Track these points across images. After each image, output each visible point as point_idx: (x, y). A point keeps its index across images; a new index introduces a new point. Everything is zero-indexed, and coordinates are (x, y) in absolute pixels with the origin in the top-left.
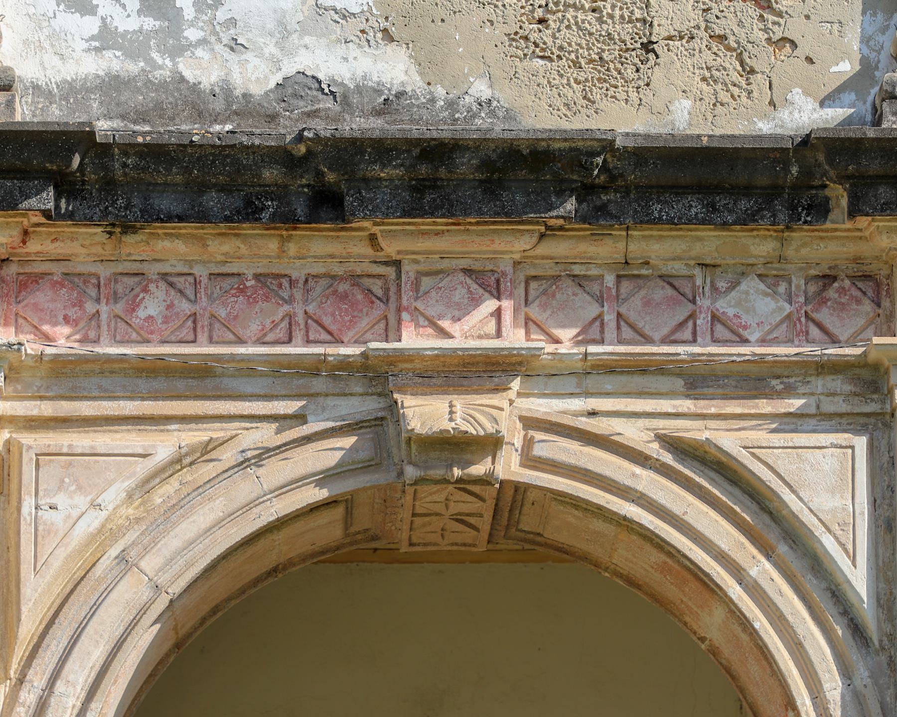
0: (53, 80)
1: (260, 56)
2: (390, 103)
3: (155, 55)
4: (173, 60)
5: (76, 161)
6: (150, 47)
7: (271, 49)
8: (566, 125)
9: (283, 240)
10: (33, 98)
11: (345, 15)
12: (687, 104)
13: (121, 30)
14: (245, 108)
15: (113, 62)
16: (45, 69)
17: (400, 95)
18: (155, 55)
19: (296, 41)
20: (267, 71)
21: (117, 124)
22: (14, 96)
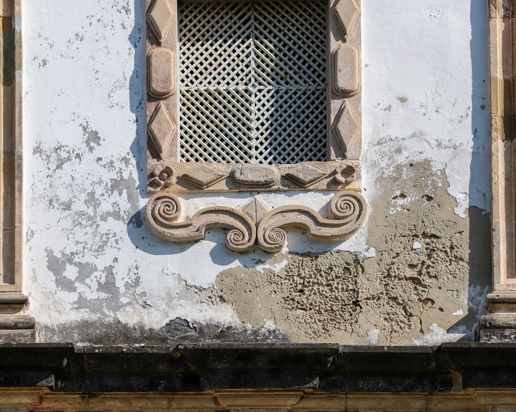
1: (158, 310)
2: (225, 332)
3: (106, 311)
4: (114, 313)
5: (65, 362)
6: (103, 307)
7: (164, 306)
8: (313, 342)
9: (170, 400)
11: (201, 289)
12: (377, 331)
13: (88, 299)
14: (151, 335)
15: (84, 315)
17: (229, 328)
18: (106, 311)
19: (176, 303)
20: (162, 317)
21: (87, 344)
22: (35, 331)
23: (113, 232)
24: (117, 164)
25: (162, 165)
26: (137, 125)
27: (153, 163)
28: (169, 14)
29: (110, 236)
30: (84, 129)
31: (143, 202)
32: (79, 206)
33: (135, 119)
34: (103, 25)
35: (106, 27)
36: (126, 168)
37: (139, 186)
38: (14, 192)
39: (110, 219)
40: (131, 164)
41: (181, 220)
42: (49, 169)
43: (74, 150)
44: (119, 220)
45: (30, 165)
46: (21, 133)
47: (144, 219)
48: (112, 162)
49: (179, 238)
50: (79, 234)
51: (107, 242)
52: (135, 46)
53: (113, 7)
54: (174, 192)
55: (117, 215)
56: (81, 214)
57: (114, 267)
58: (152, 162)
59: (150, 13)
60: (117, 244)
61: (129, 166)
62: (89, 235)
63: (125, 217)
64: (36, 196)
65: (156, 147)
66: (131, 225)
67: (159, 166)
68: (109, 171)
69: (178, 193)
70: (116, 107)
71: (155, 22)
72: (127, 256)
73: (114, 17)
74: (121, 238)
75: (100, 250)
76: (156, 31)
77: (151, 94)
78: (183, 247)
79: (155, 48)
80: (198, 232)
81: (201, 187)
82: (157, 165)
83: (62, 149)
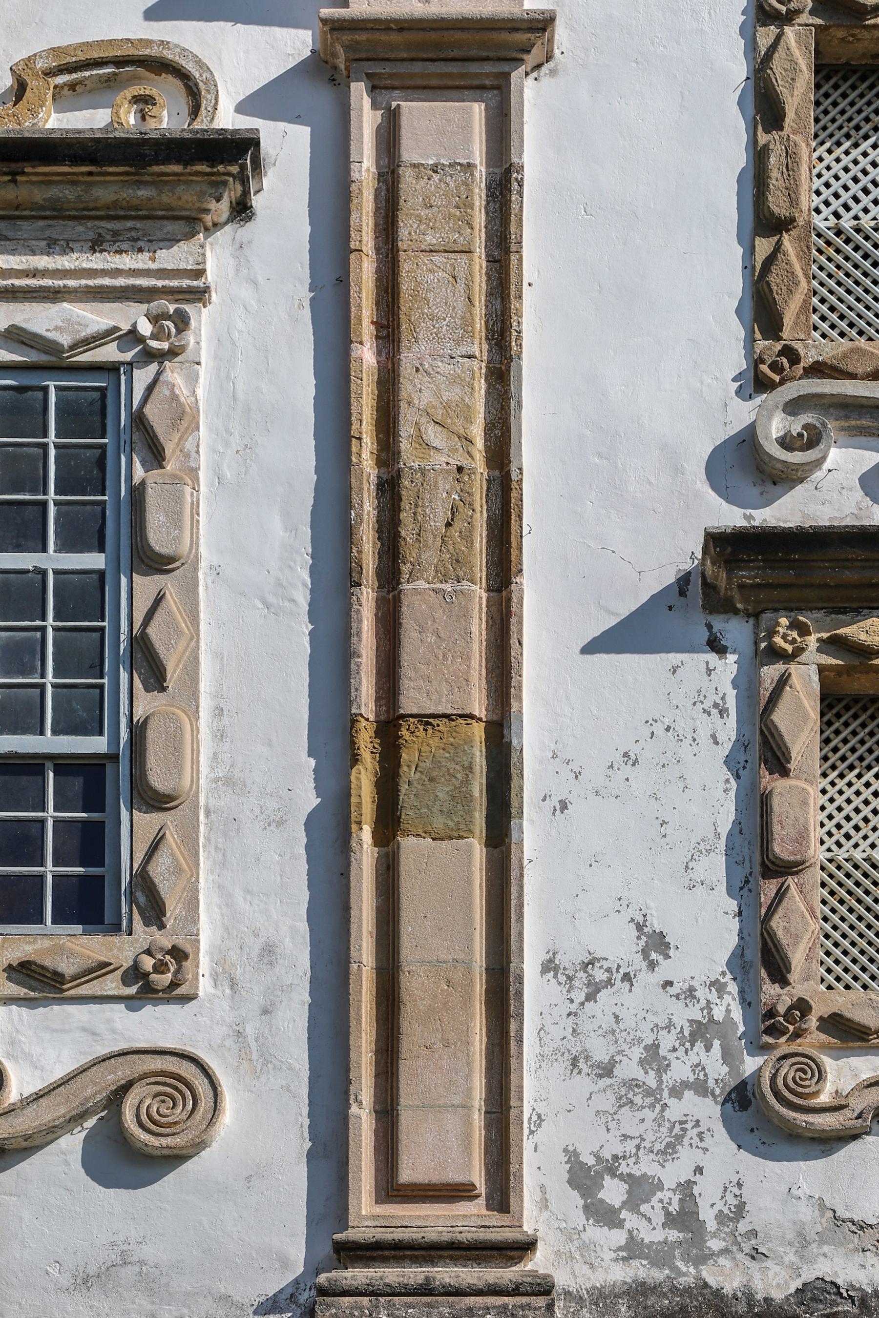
0: (583, 1287)
1: (781, 1263)
3: (680, 1264)
4: (696, 1268)
6: (674, 1257)
7: (791, 1257)
10: (565, 1303)
13: (646, 1241)
15: (640, 1270)
16: (575, 1277)
18: (680, 1264)
19: (815, 1250)
20: (787, 1277)
23: (694, 1119)
24: (702, 993)
25: (791, 996)
26: (741, 922)
27: (772, 991)
28: (806, 718)
29: (688, 1126)
30: (640, 928)
31: (751, 1064)
32: (629, 1069)
33: (737, 909)
34: (677, 738)
35: (681, 740)
36: (718, 1001)
37: (744, 1033)
38: (508, 1043)
39: (688, 1094)
40: (730, 993)
41: (824, 1098)
42: (572, 1001)
43: (619, 967)
44: (705, 1095)
45: (536, 994)
46: (521, 935)
47: (754, 1094)
48: (692, 990)
49: (823, 1130)
50: (629, 1121)
51: (683, 1136)
52: (738, 777)
53: (694, 704)
54: (812, 1046)
55: (701, 1088)
56: (633, 1084)
57: (695, 1183)
58: (770, 990)
59: (769, 715)
60: (702, 1140)
61: (725, 996)
62: (649, 1123)
63: (718, 1091)
64: (547, 1050)
65: (779, 961)
66: (729, 1105)
67: (784, 997)
68: (687, 1006)
69: (820, 1047)
70: (699, 890)
71: (779, 732)
72: (720, 1163)
73: (698, 722)
74: (709, 1130)
75: (669, 1150)
76: (780, 748)
77: (770, 865)
78: (828, 1147)
79: (777, 779)
80: (860, 1121)
81: (865, 1037)
82: (779, 996)
83: (597, 965)
